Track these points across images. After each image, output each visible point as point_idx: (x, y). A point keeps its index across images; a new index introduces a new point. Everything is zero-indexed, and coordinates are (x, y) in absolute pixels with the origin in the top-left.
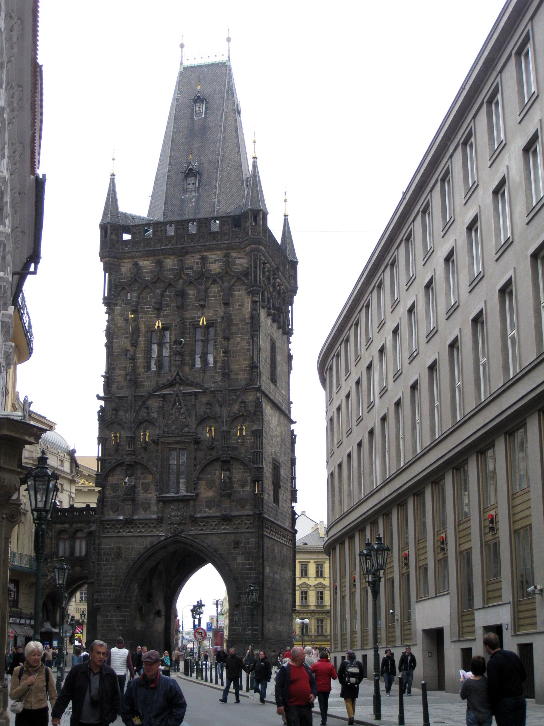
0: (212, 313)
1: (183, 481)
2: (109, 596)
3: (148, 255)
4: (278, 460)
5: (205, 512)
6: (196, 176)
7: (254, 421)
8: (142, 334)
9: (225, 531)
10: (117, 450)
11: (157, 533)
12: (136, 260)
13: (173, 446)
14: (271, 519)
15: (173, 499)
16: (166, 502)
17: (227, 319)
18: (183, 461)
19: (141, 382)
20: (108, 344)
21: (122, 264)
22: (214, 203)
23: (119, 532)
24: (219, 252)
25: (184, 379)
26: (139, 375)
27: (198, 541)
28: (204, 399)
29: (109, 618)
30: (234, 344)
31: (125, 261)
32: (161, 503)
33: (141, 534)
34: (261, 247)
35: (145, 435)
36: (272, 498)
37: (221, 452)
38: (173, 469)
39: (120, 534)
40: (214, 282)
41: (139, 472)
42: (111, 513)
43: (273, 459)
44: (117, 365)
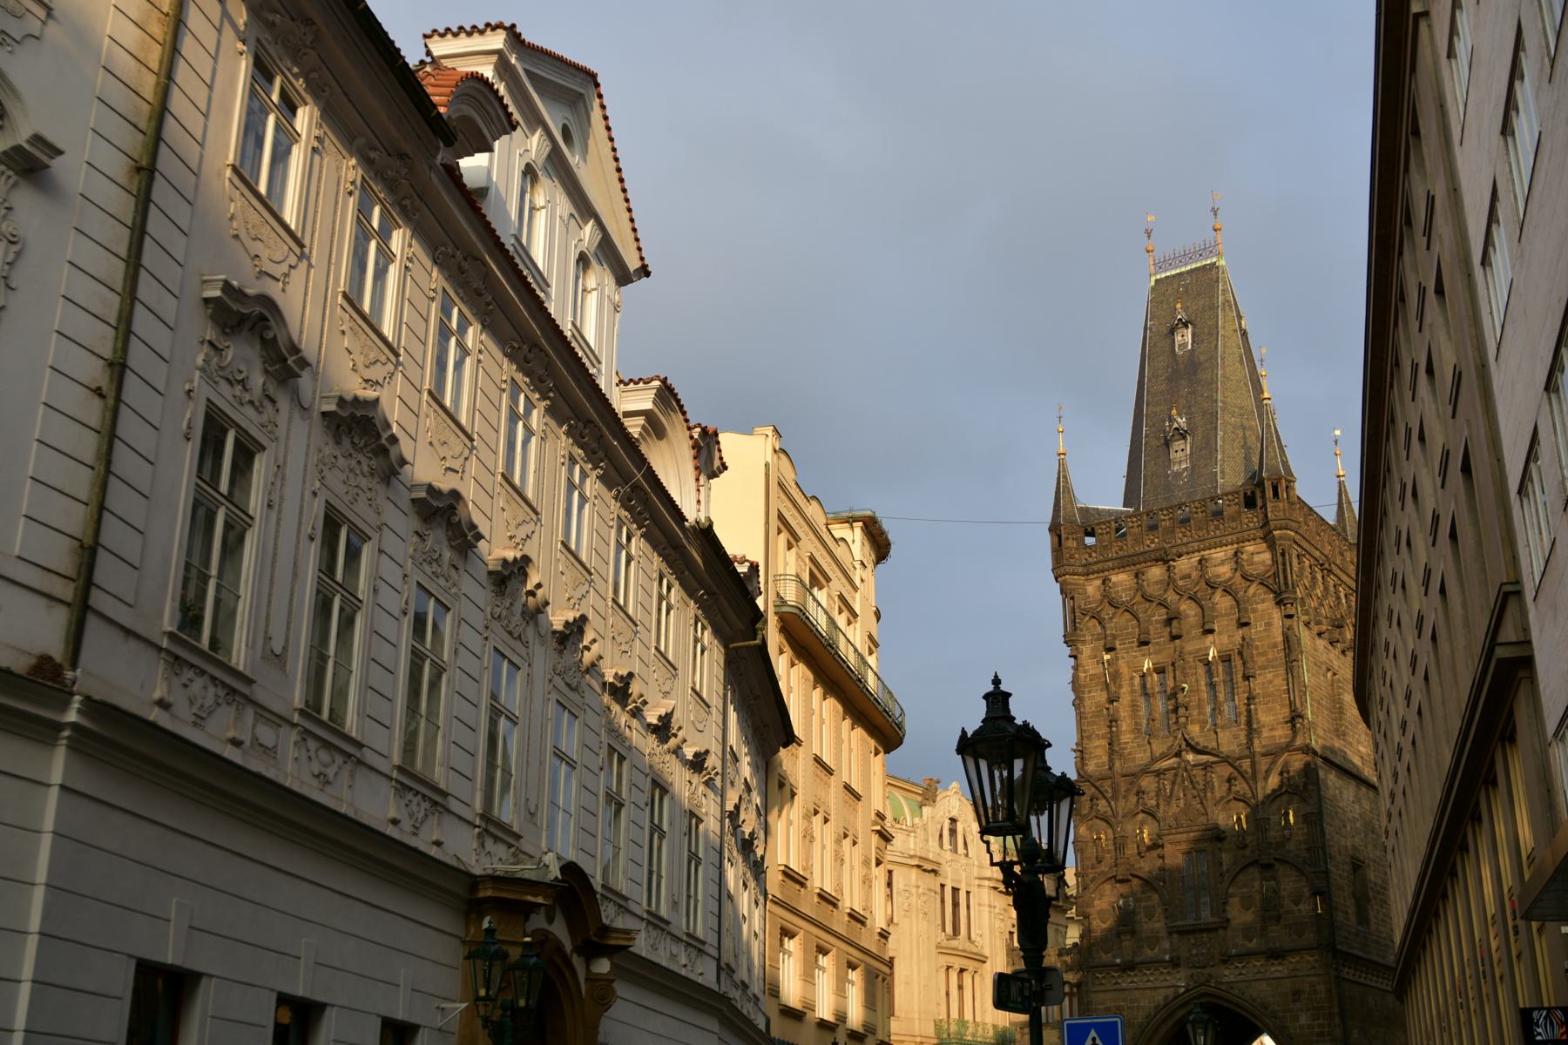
0: (1225, 639)
1: (1205, 899)
3: (1123, 563)
4: (1362, 859)
6: (1184, 438)
7: (1305, 801)
8: (1125, 683)
9: (1278, 975)
11: (1173, 981)
12: (1106, 573)
14: (1356, 952)
15: (1191, 928)
16: (1182, 932)
19: (1130, 754)
20: (1077, 702)
22: (1216, 475)
23: (1117, 983)
24: (1229, 547)
25: (1193, 743)
26: (1126, 743)
27: (1236, 992)
28: (1226, 771)
30: (1263, 683)
31: (1091, 576)
32: (1175, 936)
33: (1149, 985)
34: (1289, 532)
35: (1142, 832)
36: (1353, 918)
37: (1257, 853)
39: (1118, 986)
42: (1103, 955)
43: (1353, 857)
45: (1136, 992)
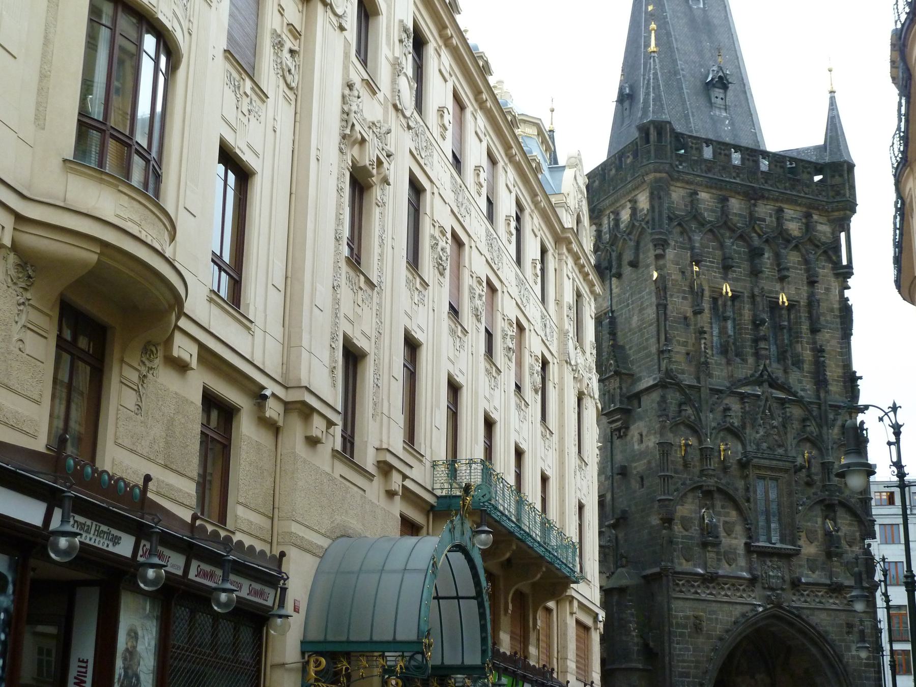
3: (712, 185)
5: (807, 576)
9: (834, 607)
11: (749, 600)
13: (763, 472)
17: (812, 303)
18: (773, 495)
23: (696, 593)
24: (798, 208)
31: (679, 184)
33: (725, 599)
38: (761, 506)
39: (697, 596)
40: (796, 247)
41: (718, 504)
42: (684, 561)
44: (675, 337)
45: (714, 604)
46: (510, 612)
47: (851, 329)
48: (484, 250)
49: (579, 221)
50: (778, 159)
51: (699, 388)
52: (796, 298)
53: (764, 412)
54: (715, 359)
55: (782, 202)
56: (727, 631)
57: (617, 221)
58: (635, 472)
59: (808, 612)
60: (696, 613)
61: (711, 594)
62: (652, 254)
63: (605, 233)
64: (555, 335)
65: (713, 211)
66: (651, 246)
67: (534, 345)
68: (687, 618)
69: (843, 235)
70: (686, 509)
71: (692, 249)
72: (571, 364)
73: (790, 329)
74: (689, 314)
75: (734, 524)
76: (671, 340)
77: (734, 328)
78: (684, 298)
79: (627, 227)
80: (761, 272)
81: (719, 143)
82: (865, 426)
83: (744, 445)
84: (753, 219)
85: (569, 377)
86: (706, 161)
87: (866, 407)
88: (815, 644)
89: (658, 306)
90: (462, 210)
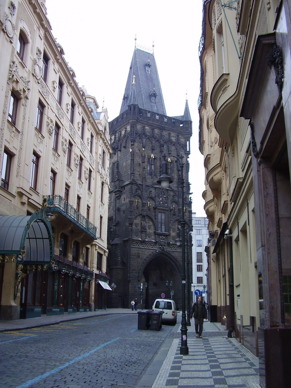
2: (135, 275)
5: (172, 242)
9: (180, 251)
10: (137, 208)
11: (154, 248)
18: (163, 218)
21: (138, 125)
23: (139, 246)
24: (175, 133)
29: (135, 286)
31: (139, 124)
38: (159, 220)
39: (139, 247)
41: (147, 220)
46: (72, 247)
47: (189, 170)
48: (68, 131)
49: (105, 129)
50: (170, 119)
51: (143, 185)
52: (173, 160)
53: (162, 193)
54: (148, 177)
55: (170, 131)
56: (147, 257)
57: (121, 134)
58: (122, 210)
59: (171, 252)
60: (138, 252)
61: (143, 246)
62: (130, 144)
63: (117, 138)
64: (95, 163)
65: (149, 132)
66: (130, 142)
67: (86, 165)
68: (135, 253)
69: (188, 142)
70: (138, 221)
71: (143, 143)
72: (99, 173)
73: (171, 169)
74: (141, 163)
75: (151, 226)
76: (135, 170)
77: (154, 168)
78: (139, 158)
79: (123, 136)
80: (163, 151)
81: (152, 112)
82: (191, 199)
83: (155, 203)
84: (162, 136)
85: (99, 177)
86: (148, 117)
87: (192, 193)
88: (173, 261)
89: (131, 160)
90: (60, 116)
